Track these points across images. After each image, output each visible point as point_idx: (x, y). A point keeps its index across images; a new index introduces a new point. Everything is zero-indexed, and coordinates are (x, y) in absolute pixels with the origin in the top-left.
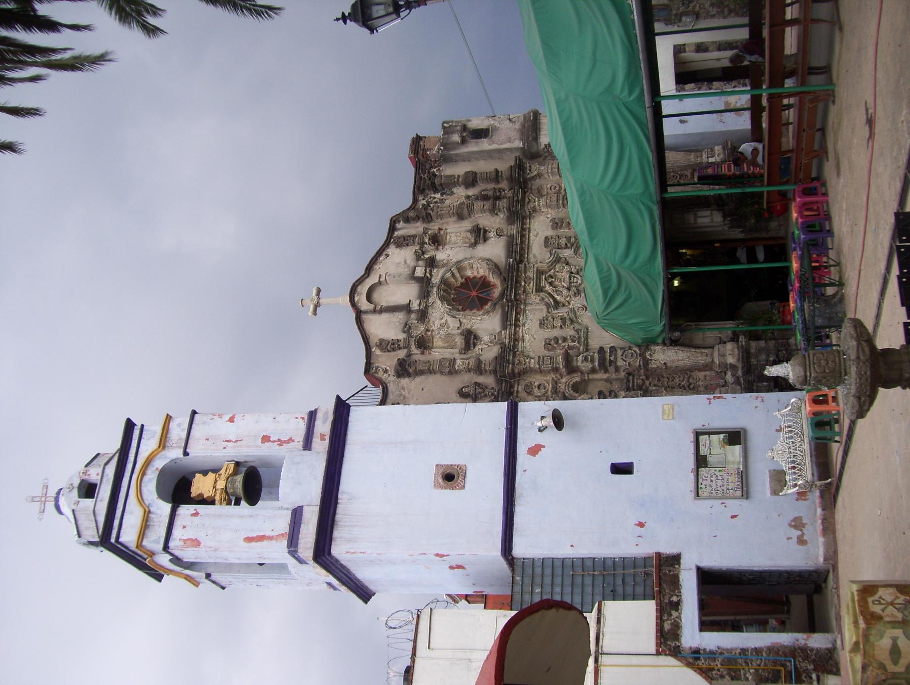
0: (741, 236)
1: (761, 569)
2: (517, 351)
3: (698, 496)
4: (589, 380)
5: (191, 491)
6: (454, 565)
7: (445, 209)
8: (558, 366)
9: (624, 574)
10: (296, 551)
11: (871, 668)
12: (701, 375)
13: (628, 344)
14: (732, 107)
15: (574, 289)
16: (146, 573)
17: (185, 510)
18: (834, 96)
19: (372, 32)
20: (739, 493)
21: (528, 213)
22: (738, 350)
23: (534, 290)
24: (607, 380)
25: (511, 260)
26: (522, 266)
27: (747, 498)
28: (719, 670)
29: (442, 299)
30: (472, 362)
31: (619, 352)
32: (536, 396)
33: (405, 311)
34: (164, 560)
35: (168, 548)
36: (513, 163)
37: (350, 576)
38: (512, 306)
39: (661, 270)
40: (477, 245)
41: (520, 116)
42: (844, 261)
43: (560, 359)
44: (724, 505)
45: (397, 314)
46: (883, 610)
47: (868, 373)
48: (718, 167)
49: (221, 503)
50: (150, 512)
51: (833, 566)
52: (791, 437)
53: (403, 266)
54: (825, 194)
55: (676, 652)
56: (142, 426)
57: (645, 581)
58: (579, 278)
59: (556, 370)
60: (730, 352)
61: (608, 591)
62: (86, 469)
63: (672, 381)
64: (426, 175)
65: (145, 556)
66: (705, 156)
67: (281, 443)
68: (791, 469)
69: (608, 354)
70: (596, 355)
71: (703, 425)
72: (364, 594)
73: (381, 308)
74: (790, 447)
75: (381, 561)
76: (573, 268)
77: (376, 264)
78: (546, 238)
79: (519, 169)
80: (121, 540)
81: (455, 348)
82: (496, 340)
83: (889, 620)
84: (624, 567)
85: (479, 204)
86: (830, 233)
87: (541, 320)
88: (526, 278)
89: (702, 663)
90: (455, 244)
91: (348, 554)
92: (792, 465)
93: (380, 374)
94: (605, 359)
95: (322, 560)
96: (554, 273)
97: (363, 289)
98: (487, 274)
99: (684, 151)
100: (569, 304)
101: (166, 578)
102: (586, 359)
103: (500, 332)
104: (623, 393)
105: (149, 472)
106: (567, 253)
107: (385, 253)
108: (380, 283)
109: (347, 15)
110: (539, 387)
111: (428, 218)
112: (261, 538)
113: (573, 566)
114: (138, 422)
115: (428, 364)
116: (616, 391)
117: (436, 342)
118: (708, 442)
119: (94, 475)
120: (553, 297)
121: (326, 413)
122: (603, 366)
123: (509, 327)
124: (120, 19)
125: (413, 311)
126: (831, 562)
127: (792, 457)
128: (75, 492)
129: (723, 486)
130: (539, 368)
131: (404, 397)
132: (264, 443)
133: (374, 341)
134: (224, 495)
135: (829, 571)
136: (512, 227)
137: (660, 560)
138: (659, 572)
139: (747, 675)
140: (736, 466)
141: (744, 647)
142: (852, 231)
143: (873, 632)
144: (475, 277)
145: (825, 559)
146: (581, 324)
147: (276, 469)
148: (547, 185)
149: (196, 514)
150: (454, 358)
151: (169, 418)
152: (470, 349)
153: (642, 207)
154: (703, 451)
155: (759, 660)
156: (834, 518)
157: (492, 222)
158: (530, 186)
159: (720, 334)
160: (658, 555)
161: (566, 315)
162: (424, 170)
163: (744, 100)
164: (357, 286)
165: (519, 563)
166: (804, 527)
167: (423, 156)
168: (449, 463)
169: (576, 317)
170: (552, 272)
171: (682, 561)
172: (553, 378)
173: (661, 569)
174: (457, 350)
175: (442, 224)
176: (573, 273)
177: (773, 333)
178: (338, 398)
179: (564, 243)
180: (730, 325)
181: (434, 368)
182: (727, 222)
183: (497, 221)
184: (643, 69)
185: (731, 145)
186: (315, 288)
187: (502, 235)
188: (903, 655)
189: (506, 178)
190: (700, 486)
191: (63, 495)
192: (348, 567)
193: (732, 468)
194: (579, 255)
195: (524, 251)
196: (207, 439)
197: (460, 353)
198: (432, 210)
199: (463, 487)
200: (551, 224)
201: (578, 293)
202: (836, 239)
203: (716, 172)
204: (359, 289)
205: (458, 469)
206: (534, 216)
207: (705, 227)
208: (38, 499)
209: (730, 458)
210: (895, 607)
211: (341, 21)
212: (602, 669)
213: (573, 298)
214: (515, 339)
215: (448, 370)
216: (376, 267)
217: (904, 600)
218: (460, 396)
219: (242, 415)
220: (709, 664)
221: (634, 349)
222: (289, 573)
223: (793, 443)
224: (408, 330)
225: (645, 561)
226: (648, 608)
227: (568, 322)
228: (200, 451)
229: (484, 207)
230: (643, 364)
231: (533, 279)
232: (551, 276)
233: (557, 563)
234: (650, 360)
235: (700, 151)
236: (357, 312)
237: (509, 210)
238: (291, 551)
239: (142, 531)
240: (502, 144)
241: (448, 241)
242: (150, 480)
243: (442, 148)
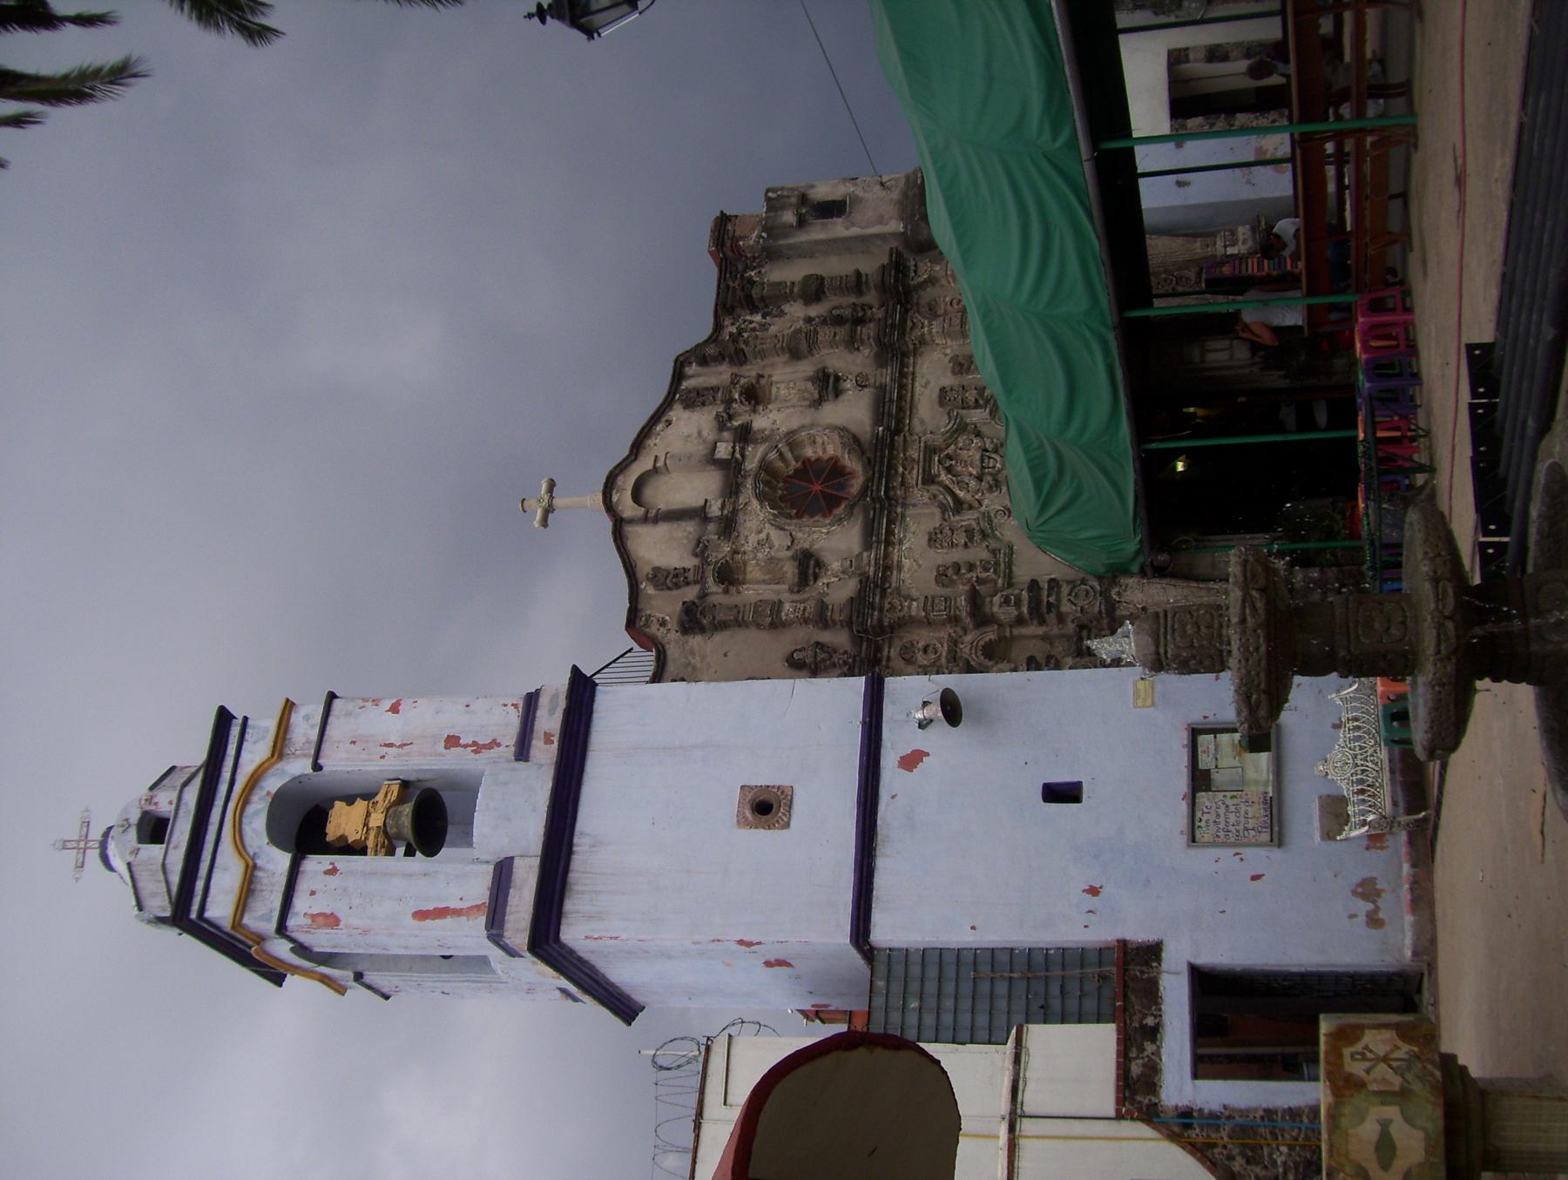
0: (1283, 383)
1: (1303, 970)
2: (890, 587)
3: (1194, 841)
4: (1013, 638)
5: (327, 831)
6: (772, 960)
7: (768, 340)
8: (958, 613)
9: (1063, 977)
10: (501, 936)
11: (1342, 1175)
13: (1081, 575)
14: (1268, 156)
15: (989, 478)
16: (256, 972)
17: (315, 864)
18: (1416, 137)
19: (591, 37)
20: (1265, 837)
21: (911, 347)
23: (920, 482)
24: (1044, 638)
25: (881, 429)
26: (899, 439)
27: (1280, 845)
28: (1225, 1147)
29: (761, 497)
30: (811, 607)
31: (1065, 589)
32: (920, 666)
33: (697, 520)
34: (281, 949)
35: (286, 928)
36: (885, 260)
37: (595, 976)
38: (882, 509)
39: (1129, 444)
40: (824, 404)
41: (899, 178)
42: (1434, 429)
43: (962, 601)
44: (1240, 856)
45: (684, 524)
46: (1368, 1071)
47: (1263, 649)
48: (1240, 264)
49: (376, 851)
50: (255, 867)
51: (1429, 965)
52: (1359, 738)
53: (695, 442)
54: (1409, 310)
55: (1150, 1114)
56: (246, 719)
57: (1099, 988)
58: (998, 458)
59: (954, 620)
61: (1035, 1006)
62: (151, 794)
64: (737, 283)
65: (250, 943)
66: (1220, 244)
67: (478, 748)
68: (1355, 793)
69: (1046, 593)
70: (1025, 594)
71: (1205, 717)
72: (624, 1007)
73: (656, 515)
74: (1355, 756)
75: (647, 952)
76: (988, 441)
77: (650, 438)
78: (943, 391)
79: (898, 270)
80: (208, 914)
81: (783, 583)
82: (852, 566)
83: (1376, 1089)
84: (1063, 966)
85: (827, 332)
86: (1416, 377)
87: (930, 534)
88: (906, 459)
89: (1195, 1134)
90: (786, 401)
91: (588, 940)
92: (1360, 787)
93: (654, 629)
94: (1040, 601)
95: (546, 951)
96: (955, 451)
97: (628, 481)
98: (839, 454)
99: (1186, 235)
100: (981, 505)
101: (290, 979)
102: (1007, 601)
103: (859, 556)
104: (1069, 661)
105: (255, 798)
106: (977, 416)
108: (655, 470)
109: (546, 7)
110: (925, 650)
111: (739, 358)
112: (441, 913)
113: (975, 963)
114: (238, 712)
115: (735, 611)
116: (1058, 657)
117: (751, 572)
118: (1212, 747)
119: (164, 803)
120: (952, 491)
121: (555, 697)
122: (1038, 612)
123: (875, 545)
124: (199, 18)
125: (710, 518)
126: (1425, 957)
127: (1359, 772)
128: (133, 834)
129: (1238, 824)
130: (926, 617)
131: (694, 668)
132: (449, 748)
133: (643, 570)
134: (381, 839)
135: (1422, 974)
136: (884, 370)
137: (1125, 953)
138: (1124, 974)
139: (1275, 1157)
140: (1261, 789)
141: (1271, 1106)
142: (1443, 376)
143: (1347, 1110)
144: (818, 460)
145: (1415, 954)
146: (998, 539)
147: (468, 789)
148: (945, 297)
149: (333, 871)
150: (780, 601)
151: (289, 706)
152: (808, 585)
153: (1088, 334)
154: (1205, 762)
155: (1296, 1130)
156: (1431, 881)
157: (849, 362)
158: (915, 300)
160: (1123, 943)
161: (974, 524)
162: (734, 274)
163: (1279, 143)
164: (617, 476)
165: (881, 958)
166: (1379, 895)
167: (732, 250)
168: (764, 783)
169: (991, 528)
170: (950, 450)
171: (1164, 955)
172: (950, 634)
173: (1127, 970)
174: (785, 587)
175: (764, 367)
176: (987, 451)
177: (1332, 554)
178: (575, 670)
179: (973, 399)
180: (1261, 539)
181: (746, 618)
183: (859, 361)
184: (1072, 93)
185: (1266, 224)
186: (546, 479)
187: (865, 386)
188: (1398, 1153)
189: (875, 285)
190: (1197, 824)
191: (113, 838)
192: (593, 963)
193: (1254, 792)
194: (1000, 419)
195: (905, 413)
196: (354, 742)
197: (791, 591)
198: (746, 343)
199: (787, 825)
200: (951, 365)
201: (996, 485)
202: (1425, 387)
203: (1237, 272)
204: (620, 480)
205: (779, 793)
206: (923, 352)
207: (1219, 368)
208: (74, 844)
209: (1251, 774)
210: (1390, 1066)
211: (536, 19)
212: (1022, 1142)
213: (987, 495)
214: (886, 567)
215: (768, 620)
216: (650, 442)
217: (1407, 1053)
218: (790, 666)
219: (412, 700)
220: (1209, 1136)
221: (1090, 583)
222: (494, 972)
223: (1361, 748)
224: (703, 552)
225: (1100, 955)
226: (1104, 1037)
227: (977, 537)
228: (340, 762)
229: (835, 336)
230: (1106, 610)
231: (918, 462)
232: (949, 457)
233: (948, 958)
234: (1119, 602)
235: (1213, 235)
236: (616, 520)
237: (878, 341)
238: (492, 935)
239: (243, 896)
240: (867, 227)
241: (773, 397)
242: (256, 813)
243: (764, 235)
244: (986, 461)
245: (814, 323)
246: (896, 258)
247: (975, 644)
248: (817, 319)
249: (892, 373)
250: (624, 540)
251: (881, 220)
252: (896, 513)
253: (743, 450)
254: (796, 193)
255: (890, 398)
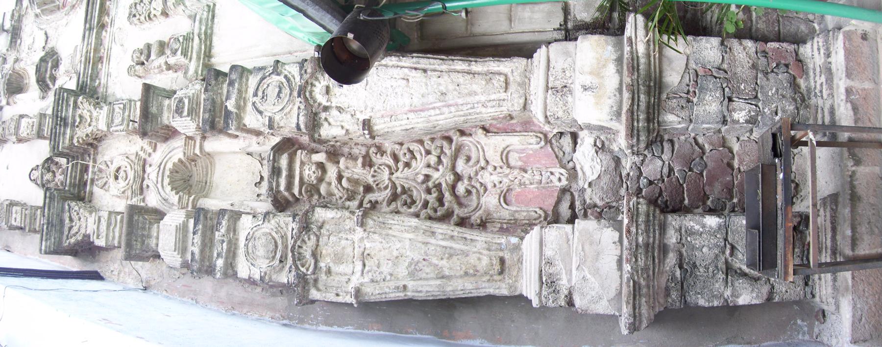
12: (493, 145)
22: (620, 72)
60: (588, 80)
63: (407, 165)
234: (326, 109)
247: (162, 167)
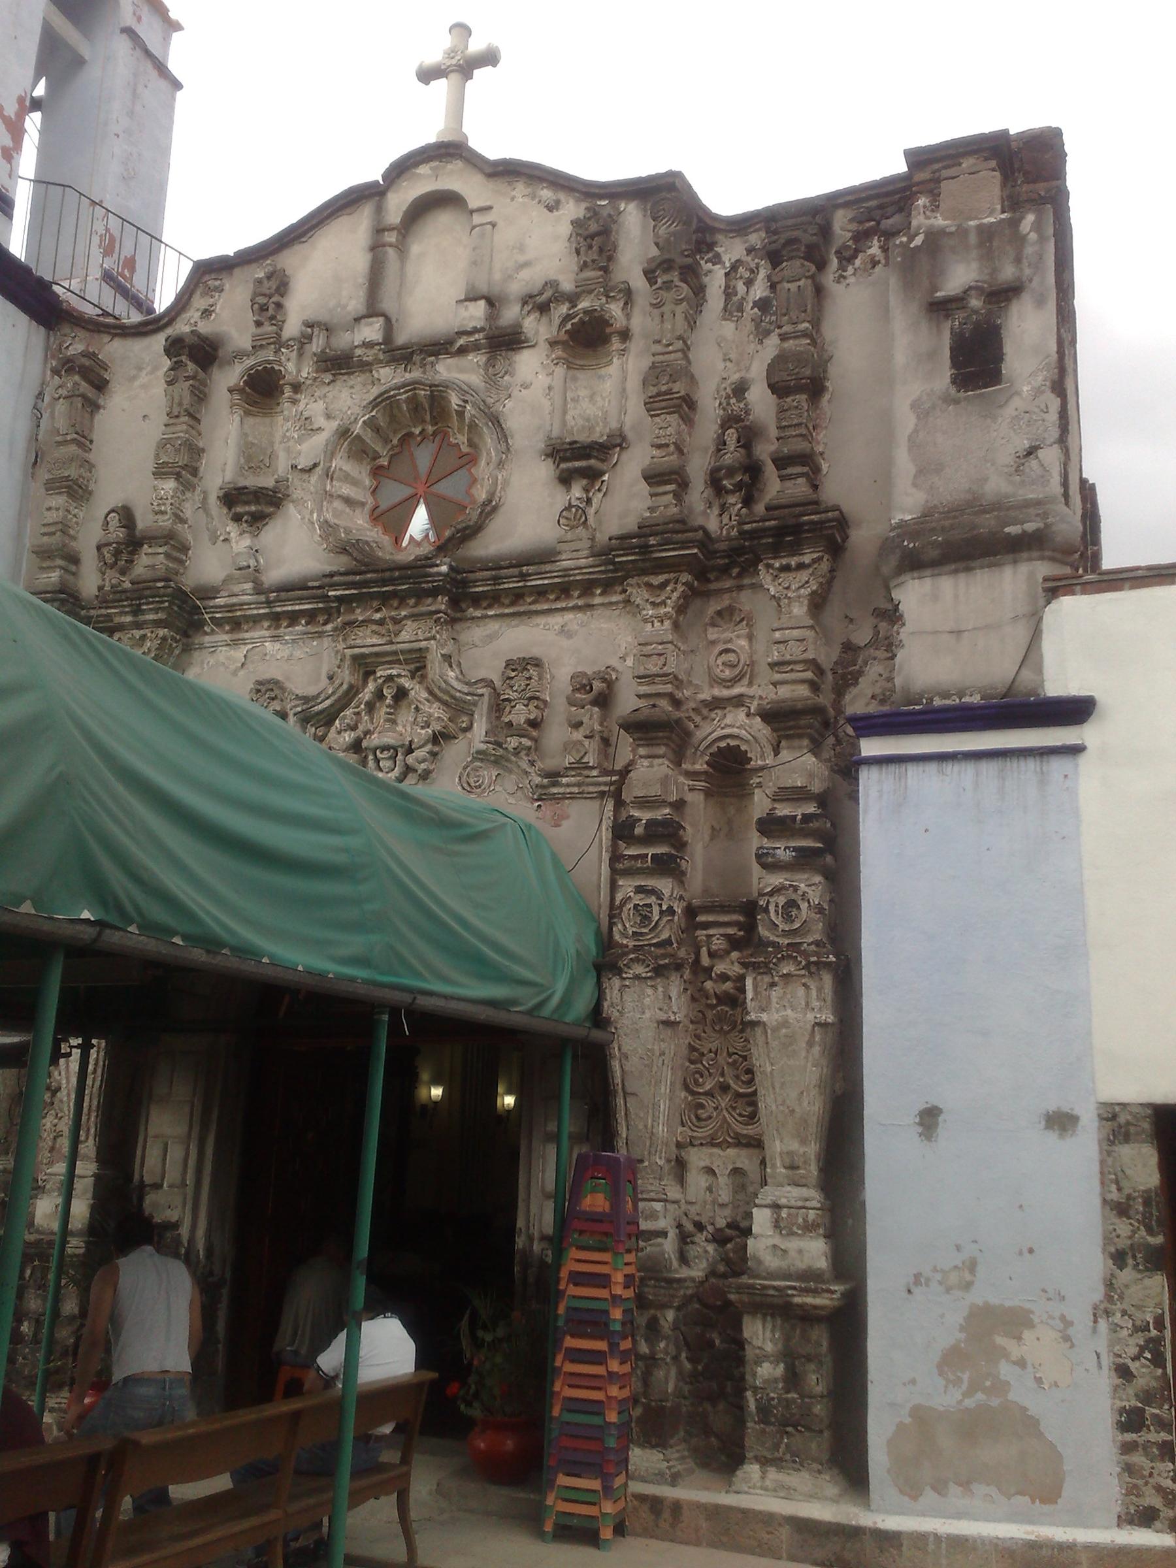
23: (357, 651)
29: (384, 402)
40: (550, 461)
66: (790, 1195)
78: (537, 663)
93: (199, 302)
97: (453, 179)
107: (562, 196)
123: (262, 598)
159: (170, 1186)
164: (461, 157)
182: (536, 1247)
195: (512, 604)
214: (236, 623)
216: (520, 189)
232: (401, 695)
241: (603, 371)
243: (918, 240)
244: (386, 754)
245: (733, 401)
246: (812, 522)
248: (742, 405)
249: (581, 568)
250: (348, 210)
251: (926, 470)
252: (325, 624)
253: (476, 347)
254: (1028, 271)
255: (530, 575)
